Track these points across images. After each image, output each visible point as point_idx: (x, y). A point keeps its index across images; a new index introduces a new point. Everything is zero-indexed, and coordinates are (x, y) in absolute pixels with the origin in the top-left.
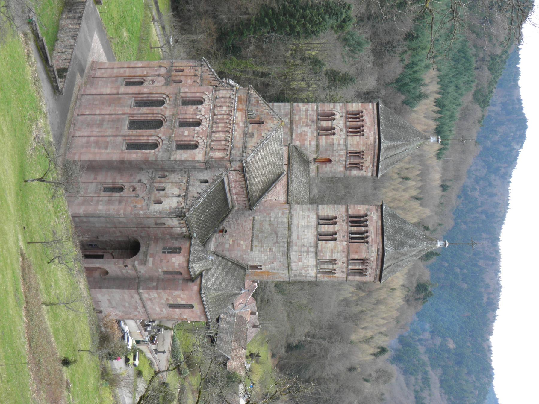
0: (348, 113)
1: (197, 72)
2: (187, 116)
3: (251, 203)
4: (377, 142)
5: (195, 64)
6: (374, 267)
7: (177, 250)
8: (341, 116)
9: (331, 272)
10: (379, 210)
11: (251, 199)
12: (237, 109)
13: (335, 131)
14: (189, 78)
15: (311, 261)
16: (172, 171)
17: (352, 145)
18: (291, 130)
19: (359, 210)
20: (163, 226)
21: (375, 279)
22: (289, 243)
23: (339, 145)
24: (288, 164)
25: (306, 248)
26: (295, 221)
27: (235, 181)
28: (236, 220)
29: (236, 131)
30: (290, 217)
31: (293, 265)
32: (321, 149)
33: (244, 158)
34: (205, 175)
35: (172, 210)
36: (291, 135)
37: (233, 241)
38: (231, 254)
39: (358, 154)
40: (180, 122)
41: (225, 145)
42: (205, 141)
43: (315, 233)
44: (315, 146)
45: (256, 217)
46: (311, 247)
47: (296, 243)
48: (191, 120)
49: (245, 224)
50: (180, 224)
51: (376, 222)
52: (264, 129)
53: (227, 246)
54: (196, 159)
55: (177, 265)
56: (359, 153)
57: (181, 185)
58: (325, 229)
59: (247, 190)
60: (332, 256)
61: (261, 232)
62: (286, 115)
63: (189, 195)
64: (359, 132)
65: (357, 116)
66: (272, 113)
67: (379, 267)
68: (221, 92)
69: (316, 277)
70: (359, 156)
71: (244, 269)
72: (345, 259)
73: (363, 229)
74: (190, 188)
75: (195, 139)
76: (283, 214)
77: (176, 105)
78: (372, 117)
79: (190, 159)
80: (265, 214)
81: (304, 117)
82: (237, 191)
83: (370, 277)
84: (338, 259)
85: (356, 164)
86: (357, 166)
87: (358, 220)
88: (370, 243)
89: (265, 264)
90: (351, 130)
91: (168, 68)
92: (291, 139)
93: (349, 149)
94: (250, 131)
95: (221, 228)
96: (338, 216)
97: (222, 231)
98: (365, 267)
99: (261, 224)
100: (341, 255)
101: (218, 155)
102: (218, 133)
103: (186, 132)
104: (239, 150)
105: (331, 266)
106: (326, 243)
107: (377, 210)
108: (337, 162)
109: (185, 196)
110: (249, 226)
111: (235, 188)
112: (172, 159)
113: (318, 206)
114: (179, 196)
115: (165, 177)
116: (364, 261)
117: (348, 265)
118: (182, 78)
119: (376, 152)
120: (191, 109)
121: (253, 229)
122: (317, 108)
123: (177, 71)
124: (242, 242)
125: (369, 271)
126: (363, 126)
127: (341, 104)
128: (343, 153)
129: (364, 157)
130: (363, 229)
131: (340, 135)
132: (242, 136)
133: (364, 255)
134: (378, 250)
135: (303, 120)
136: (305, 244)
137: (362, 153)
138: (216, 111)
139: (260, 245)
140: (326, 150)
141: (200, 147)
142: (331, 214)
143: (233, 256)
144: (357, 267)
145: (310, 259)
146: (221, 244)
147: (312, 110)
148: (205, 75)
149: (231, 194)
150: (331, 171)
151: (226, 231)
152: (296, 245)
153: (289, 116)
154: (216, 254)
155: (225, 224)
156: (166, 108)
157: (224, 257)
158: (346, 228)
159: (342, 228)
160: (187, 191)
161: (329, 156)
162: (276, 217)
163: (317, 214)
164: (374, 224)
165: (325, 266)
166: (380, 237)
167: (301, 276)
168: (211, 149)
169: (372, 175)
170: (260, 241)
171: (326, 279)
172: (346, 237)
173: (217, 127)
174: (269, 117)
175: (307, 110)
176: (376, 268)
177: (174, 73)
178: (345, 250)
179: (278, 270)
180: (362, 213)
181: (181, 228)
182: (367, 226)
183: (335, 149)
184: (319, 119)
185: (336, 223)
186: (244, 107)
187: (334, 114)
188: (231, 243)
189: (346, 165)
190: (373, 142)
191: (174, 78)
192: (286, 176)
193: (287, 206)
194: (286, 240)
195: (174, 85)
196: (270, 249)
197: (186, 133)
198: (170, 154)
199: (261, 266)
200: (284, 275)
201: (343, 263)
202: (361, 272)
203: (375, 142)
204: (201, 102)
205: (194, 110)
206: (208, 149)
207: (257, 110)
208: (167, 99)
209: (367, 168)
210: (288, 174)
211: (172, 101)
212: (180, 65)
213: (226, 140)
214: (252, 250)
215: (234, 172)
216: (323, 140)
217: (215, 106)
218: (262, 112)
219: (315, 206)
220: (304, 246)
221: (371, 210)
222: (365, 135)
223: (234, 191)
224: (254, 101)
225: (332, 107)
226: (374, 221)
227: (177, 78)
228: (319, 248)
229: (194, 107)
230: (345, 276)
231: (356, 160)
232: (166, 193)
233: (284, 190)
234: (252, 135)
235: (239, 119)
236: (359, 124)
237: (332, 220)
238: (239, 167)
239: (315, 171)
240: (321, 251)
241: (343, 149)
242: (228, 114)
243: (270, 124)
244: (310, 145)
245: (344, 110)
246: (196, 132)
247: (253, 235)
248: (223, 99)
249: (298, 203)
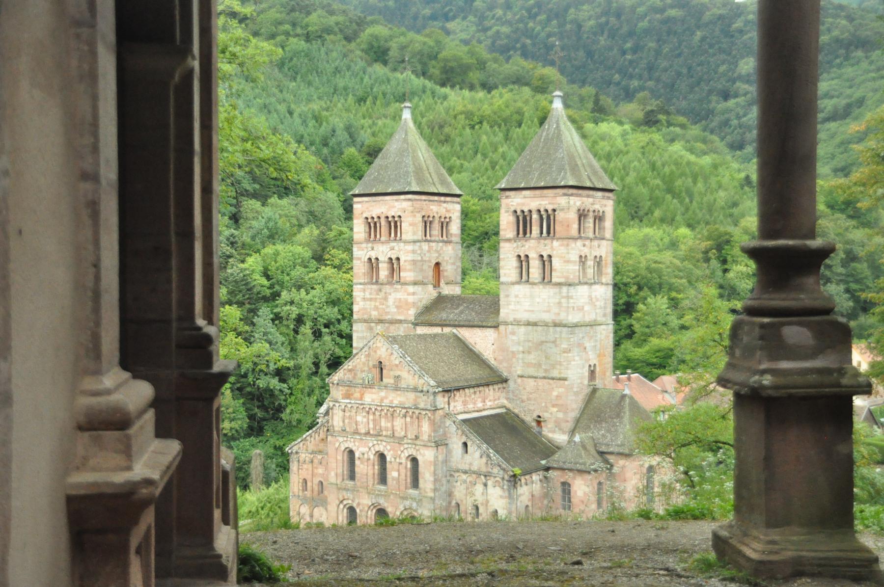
0: (368, 240)
1: (307, 459)
2: (371, 472)
3: (498, 379)
4: (410, 196)
5: (296, 463)
6: (591, 200)
7: (566, 487)
8: (373, 249)
9: (599, 261)
10: (508, 193)
11: (491, 379)
12: (361, 399)
13: (394, 257)
14: (315, 471)
15: (583, 290)
16: (450, 494)
17: (414, 233)
19: (508, 223)
20: (530, 508)
21: (609, 198)
22: (556, 325)
23: (414, 252)
24: (442, 326)
25: (563, 300)
26: (524, 316)
27: (465, 403)
28: (523, 401)
29: (391, 402)
30: (517, 323)
31: (588, 319)
32: (420, 278)
33: (431, 390)
34: (455, 446)
35: (507, 494)
37: (553, 406)
38: (573, 410)
39: (427, 223)
40: (378, 484)
41: (412, 417)
42: (406, 446)
43: (541, 287)
44: (416, 287)
45: (519, 373)
46: (560, 293)
47: (555, 314)
48: (376, 467)
49: (528, 389)
50: (526, 484)
51: (525, 197)
52: (389, 360)
53: (560, 415)
54: (432, 459)
55: (587, 490)
56: (425, 223)
57: (470, 482)
59: (478, 386)
60: (575, 262)
61: (540, 365)
62: (371, 329)
63: (484, 469)
64: (396, 222)
65: (372, 225)
66: (366, 349)
67: (591, 192)
68: (335, 423)
69: (607, 284)
70: (431, 222)
71: (594, 391)
72: (579, 243)
73: (535, 216)
74: (475, 468)
75: (403, 461)
76: (513, 333)
77: (354, 490)
78: (373, 204)
79: (432, 468)
80: (514, 360)
81: (373, 303)
82: (480, 400)
83: (605, 206)
84: (578, 252)
85: (442, 227)
86: (444, 225)
87: (523, 222)
88: (555, 207)
89: (588, 360)
90: (393, 235)
91: (300, 502)
92: (405, 321)
93: (420, 238)
94: (392, 381)
95: (534, 424)
97: (539, 423)
98: (591, 214)
99: (529, 365)
100: (573, 249)
101: (426, 427)
102: (395, 428)
103: (392, 474)
104: (420, 397)
105: (590, 263)
107: (507, 197)
108: (440, 255)
109: (485, 476)
110: (531, 382)
111: (475, 403)
112: (431, 494)
113: (502, 283)
114: (485, 485)
115: (458, 505)
116: (582, 215)
117: (588, 238)
118: (316, 481)
119: (424, 197)
120: (360, 467)
121: (536, 378)
122: (361, 284)
123: (305, 488)
124: (555, 393)
125: (597, 207)
126: (387, 217)
127: (355, 249)
128: (425, 246)
129: (431, 215)
130: (535, 216)
131: (400, 250)
132: (399, 392)
133: (573, 216)
134: (565, 195)
135: (377, 304)
136: (557, 301)
137: (426, 219)
138: (363, 431)
139: (558, 367)
140: (422, 270)
141: (414, 454)
142: (514, 263)
143: (574, 406)
144: (592, 225)
145: (579, 294)
146: (558, 424)
147: (364, 291)
148: (311, 447)
149: (484, 410)
150: (453, 264)
151: (539, 417)
152: (559, 314)
153: (373, 325)
154: (573, 432)
155: (529, 419)
156: (359, 504)
157: (578, 421)
158: (533, 241)
159: (532, 247)
160: (478, 474)
161: (430, 267)
162: (519, 343)
163: (513, 284)
164: (527, 200)
165: (590, 272)
166: (546, 191)
167: (605, 308)
168: (417, 438)
169: (459, 203)
170: (553, 367)
171: (609, 271)
172: (546, 242)
173: (387, 430)
174: (372, 353)
175: (364, 299)
176: (592, 197)
177: (308, 493)
178: (565, 242)
179: (596, 341)
180: (512, 219)
181: (532, 482)
182: (530, 211)
183: (419, 258)
184: (377, 282)
185: (527, 256)
186: (357, 390)
187: (370, 259)
188: (555, 409)
189: (443, 241)
190: (410, 203)
191: (316, 493)
192: (459, 329)
193: (502, 328)
194: (551, 329)
195: (326, 493)
196: (564, 352)
197: (395, 474)
198: (426, 497)
199: (590, 366)
200: (604, 332)
201: (584, 245)
202: (599, 218)
203: (409, 200)
204: (351, 453)
205: (362, 463)
206: (418, 442)
207: (362, 371)
208: (345, 502)
209: (448, 211)
210: (455, 326)
211: (349, 495)
212: (296, 485)
213: (405, 416)
214: (565, 379)
215: (452, 404)
216: (407, 275)
217: (356, 432)
218: (364, 364)
219: (501, 287)
220: (560, 303)
221: (507, 205)
222: (399, 214)
223: (480, 405)
224: (349, 376)
225: (359, 262)
226: (523, 201)
227: (316, 488)
228: (562, 280)
229: (357, 462)
230: (604, 242)
231: (436, 226)
232: (482, 504)
233: (477, 331)
235: (374, 396)
236: (383, 222)
237: (523, 261)
238: (444, 396)
239: (451, 287)
240: (567, 278)
241: (420, 247)
242: (368, 413)
243: (383, 350)
244: (414, 294)
245: (364, 245)
246: (393, 460)
247: (544, 378)
248: (347, 421)
249: (497, 312)
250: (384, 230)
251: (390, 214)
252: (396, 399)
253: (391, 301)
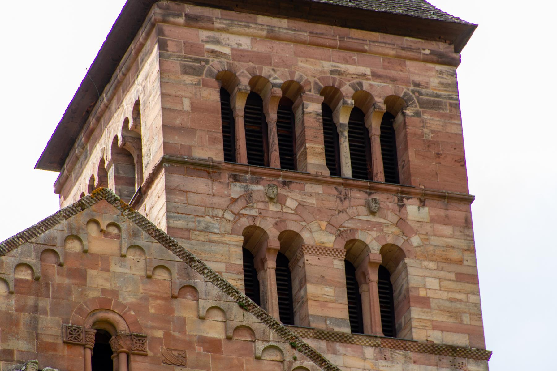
10: (189, 9)
52: (166, 317)
88: (403, 90)
96: (245, 222)
106: (425, 302)
130: (313, 108)
180: (213, 96)
226: (262, 48)
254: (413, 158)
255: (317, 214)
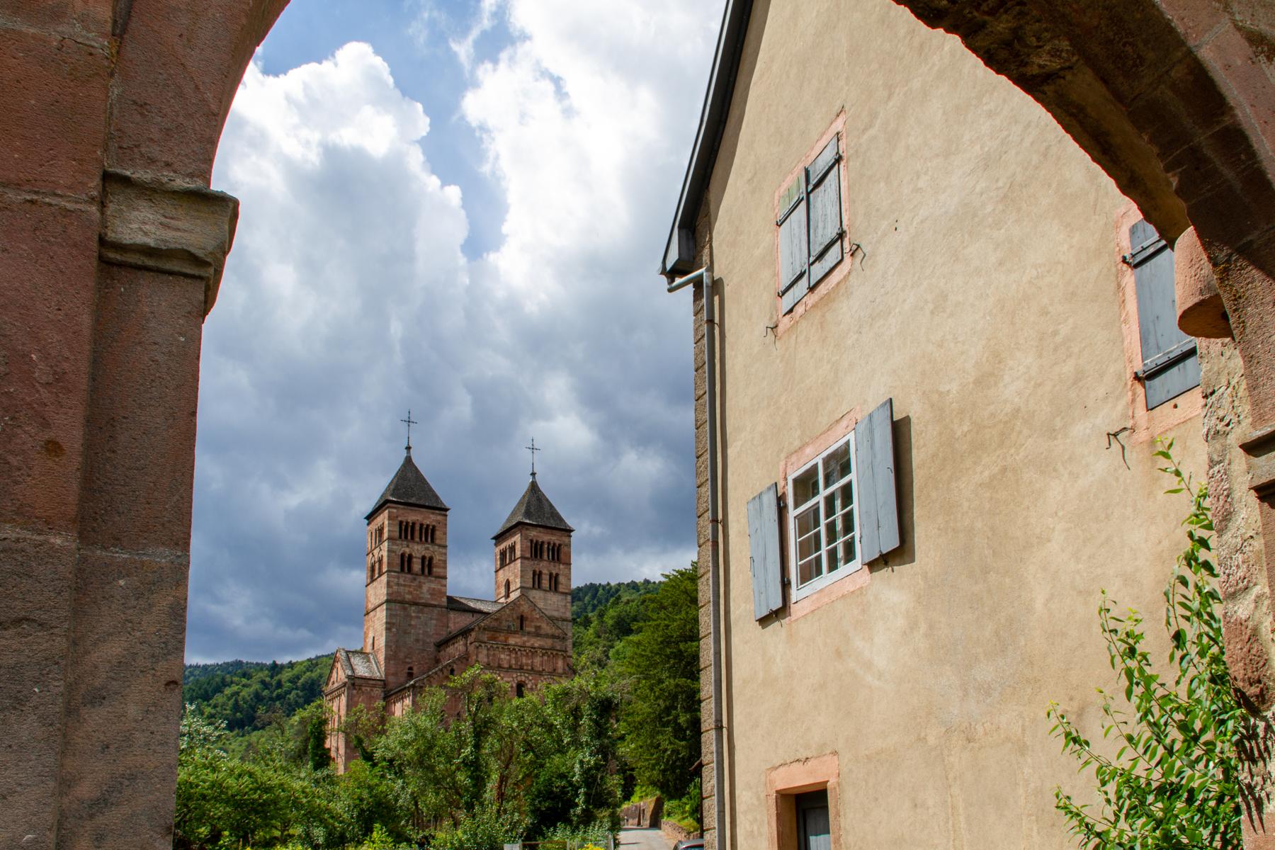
18: (426, 605)
36: (435, 606)
58: (545, 583)
62: (405, 609)
126: (422, 525)
138: (506, 666)
175: (398, 584)
187: (403, 555)
224: (495, 624)
234: (538, 628)
236: (417, 528)
237: (537, 576)
250: (417, 534)
251: (427, 522)
252: (537, 643)
253: (425, 588)
254: (562, 556)
255: (545, 567)
